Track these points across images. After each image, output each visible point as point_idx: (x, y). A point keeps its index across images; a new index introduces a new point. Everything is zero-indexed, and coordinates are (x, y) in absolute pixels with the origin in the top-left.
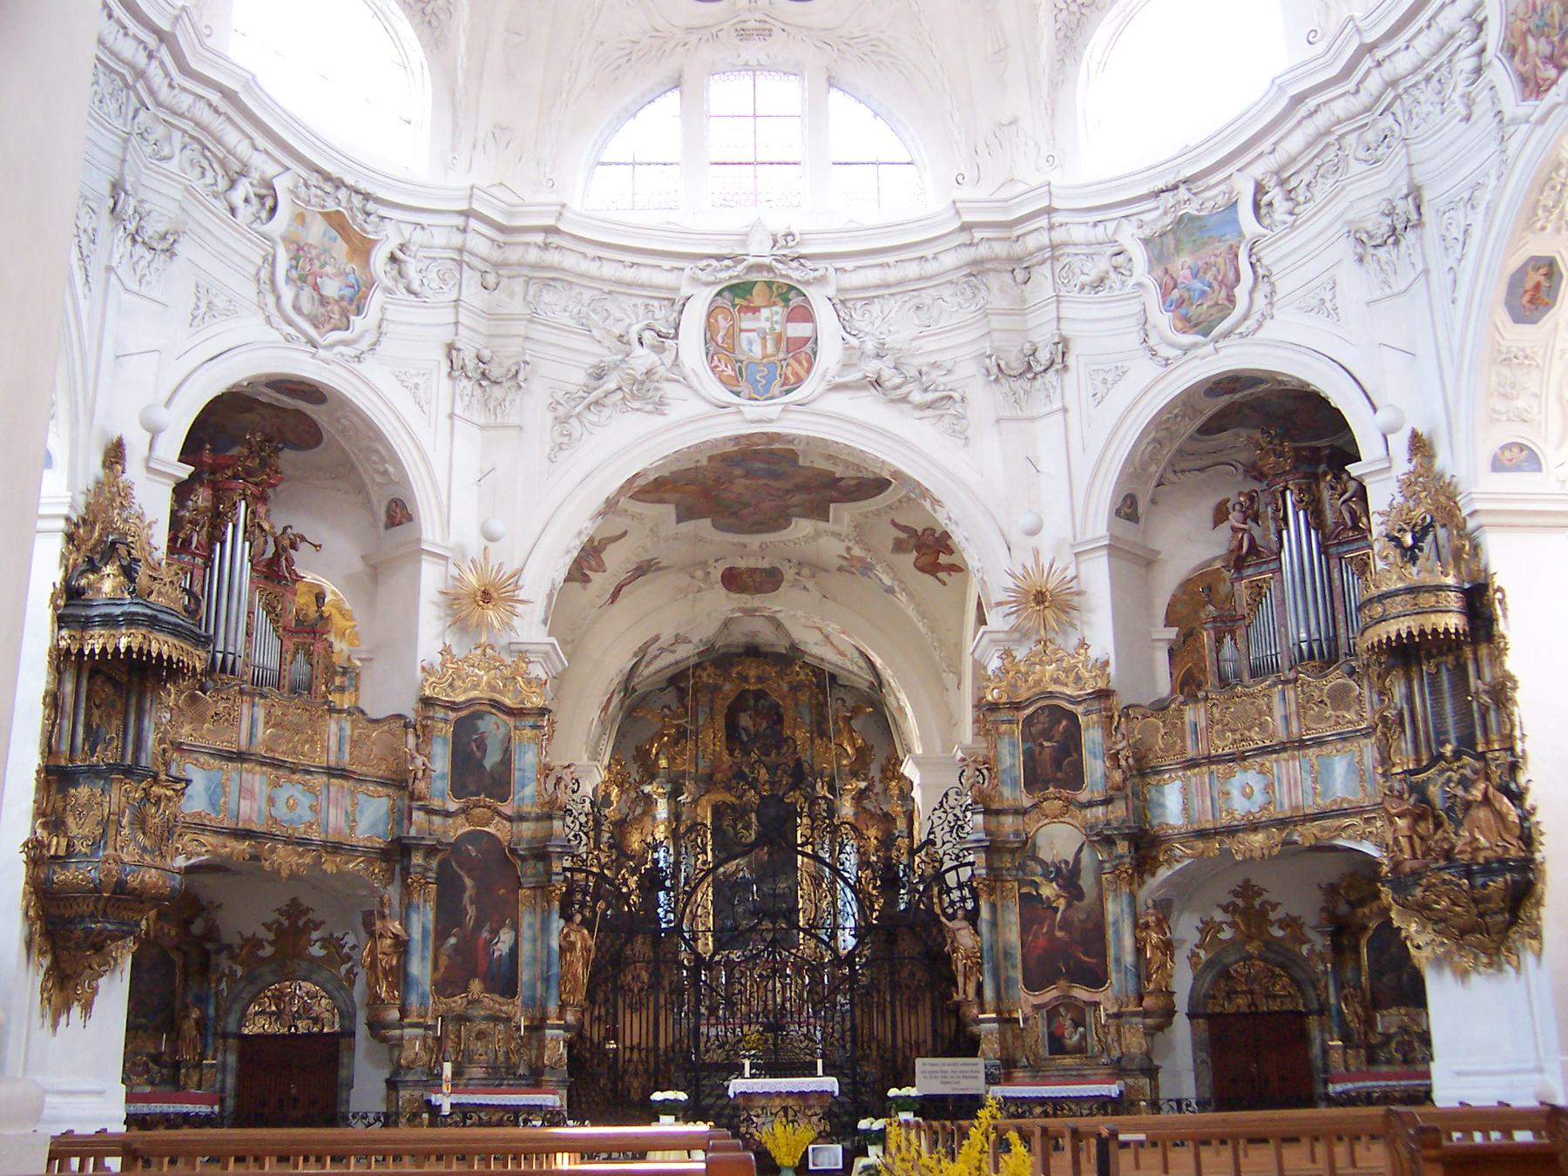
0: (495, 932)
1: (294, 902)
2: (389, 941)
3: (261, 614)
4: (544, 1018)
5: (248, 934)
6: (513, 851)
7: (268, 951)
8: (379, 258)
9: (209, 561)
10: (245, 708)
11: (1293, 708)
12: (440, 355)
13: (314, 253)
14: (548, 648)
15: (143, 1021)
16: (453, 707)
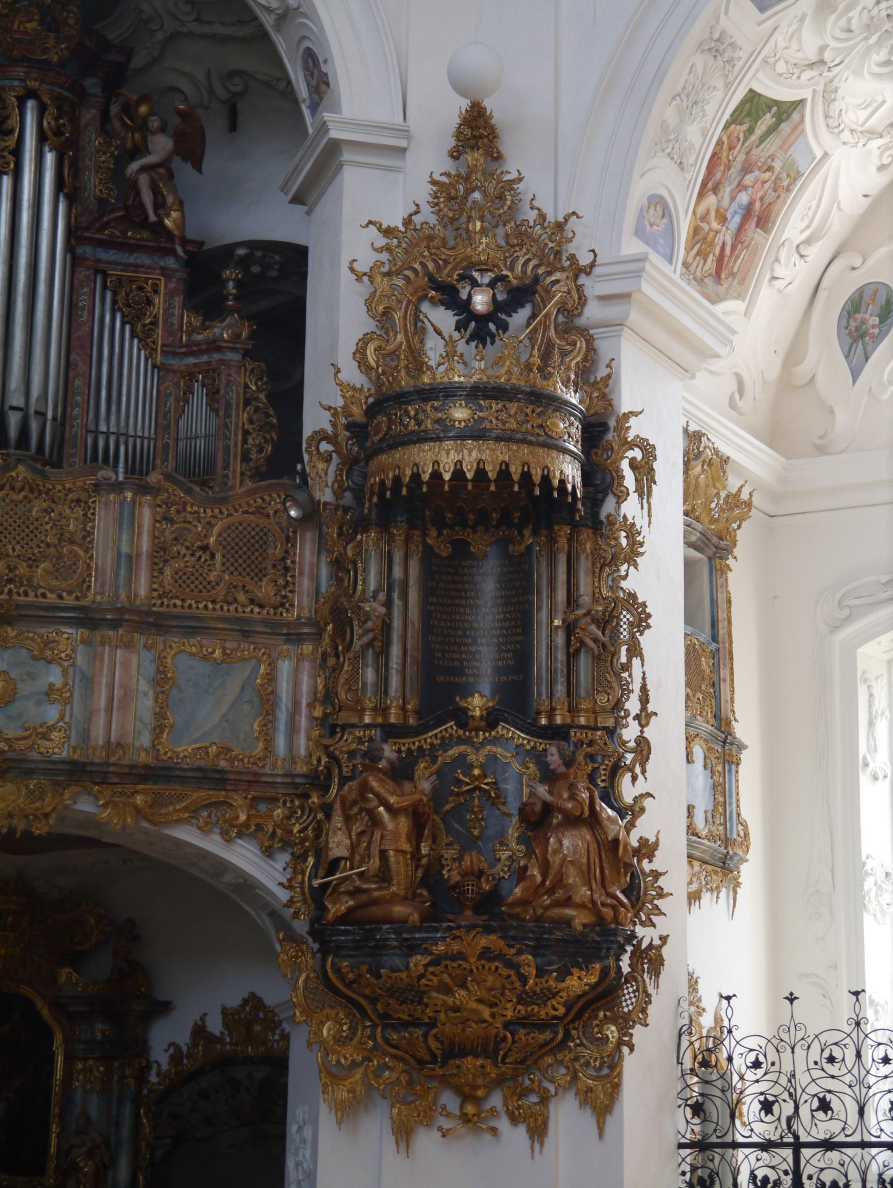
11: (145, 544)
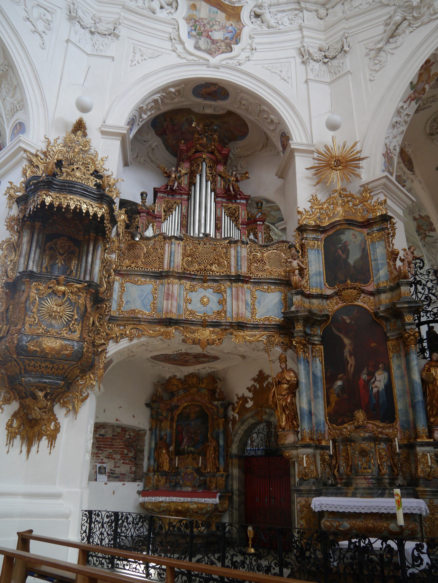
0: (371, 375)
1: (261, 373)
2: (285, 386)
3: (226, 221)
4: (417, 436)
5: (240, 395)
6: (376, 314)
7: (250, 404)
8: (245, 15)
9: (189, 195)
10: (167, 245)
12: (294, 53)
13: (205, 21)
14: (384, 180)
15: (192, 449)
16: (318, 229)
